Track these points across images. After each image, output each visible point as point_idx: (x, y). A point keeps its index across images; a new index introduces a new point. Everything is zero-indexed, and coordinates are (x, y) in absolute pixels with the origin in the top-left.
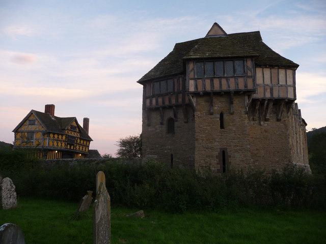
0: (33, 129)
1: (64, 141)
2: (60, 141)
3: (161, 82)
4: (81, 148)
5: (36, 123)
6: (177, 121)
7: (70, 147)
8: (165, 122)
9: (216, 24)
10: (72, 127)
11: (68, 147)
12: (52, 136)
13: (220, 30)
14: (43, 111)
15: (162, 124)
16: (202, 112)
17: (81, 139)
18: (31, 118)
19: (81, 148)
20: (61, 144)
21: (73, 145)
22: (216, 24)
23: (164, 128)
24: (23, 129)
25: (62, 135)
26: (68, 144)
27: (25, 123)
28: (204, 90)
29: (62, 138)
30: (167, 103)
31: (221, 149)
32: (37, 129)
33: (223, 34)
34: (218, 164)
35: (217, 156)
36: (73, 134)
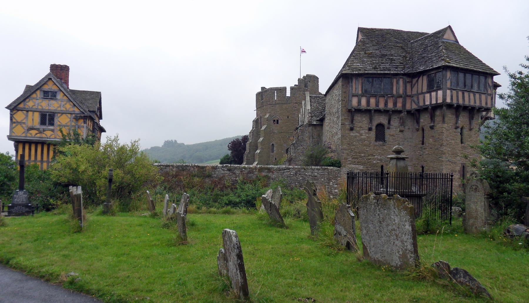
3: (375, 79)
6: (389, 128)
8: (374, 128)
9: (450, 27)
13: (452, 35)
15: (370, 129)
16: (449, 125)
22: (450, 27)
23: (373, 134)
27: (34, 96)
28: (457, 102)
30: (381, 106)
31: (462, 163)
33: (454, 40)
34: (459, 178)
35: (459, 171)
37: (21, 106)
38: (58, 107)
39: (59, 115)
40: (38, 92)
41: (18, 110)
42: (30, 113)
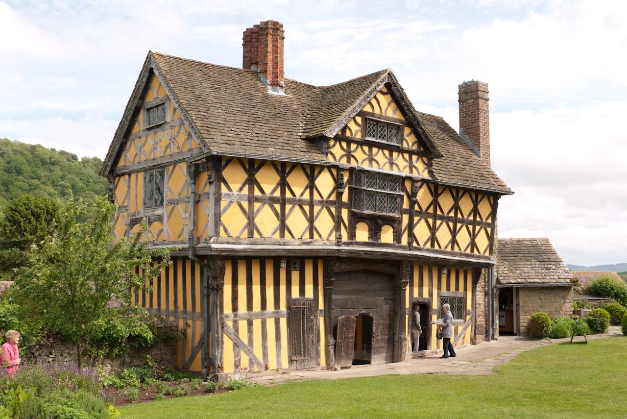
0: (159, 153)
1: (326, 204)
2: (301, 203)
4: (463, 238)
5: (168, 119)
7: (375, 232)
10: (370, 122)
11: (362, 234)
12: (235, 177)
14: (235, 59)
17: (436, 188)
18: (152, 98)
19: (444, 235)
20: (311, 220)
21: (390, 221)
24: (129, 157)
25: (311, 172)
26: (356, 218)
29: (312, 186)
32: (174, 150)
36: (381, 163)
37: (121, 163)
38: (167, 147)
39: (171, 168)
40: (142, 116)
41: (120, 176)
42: (133, 176)
